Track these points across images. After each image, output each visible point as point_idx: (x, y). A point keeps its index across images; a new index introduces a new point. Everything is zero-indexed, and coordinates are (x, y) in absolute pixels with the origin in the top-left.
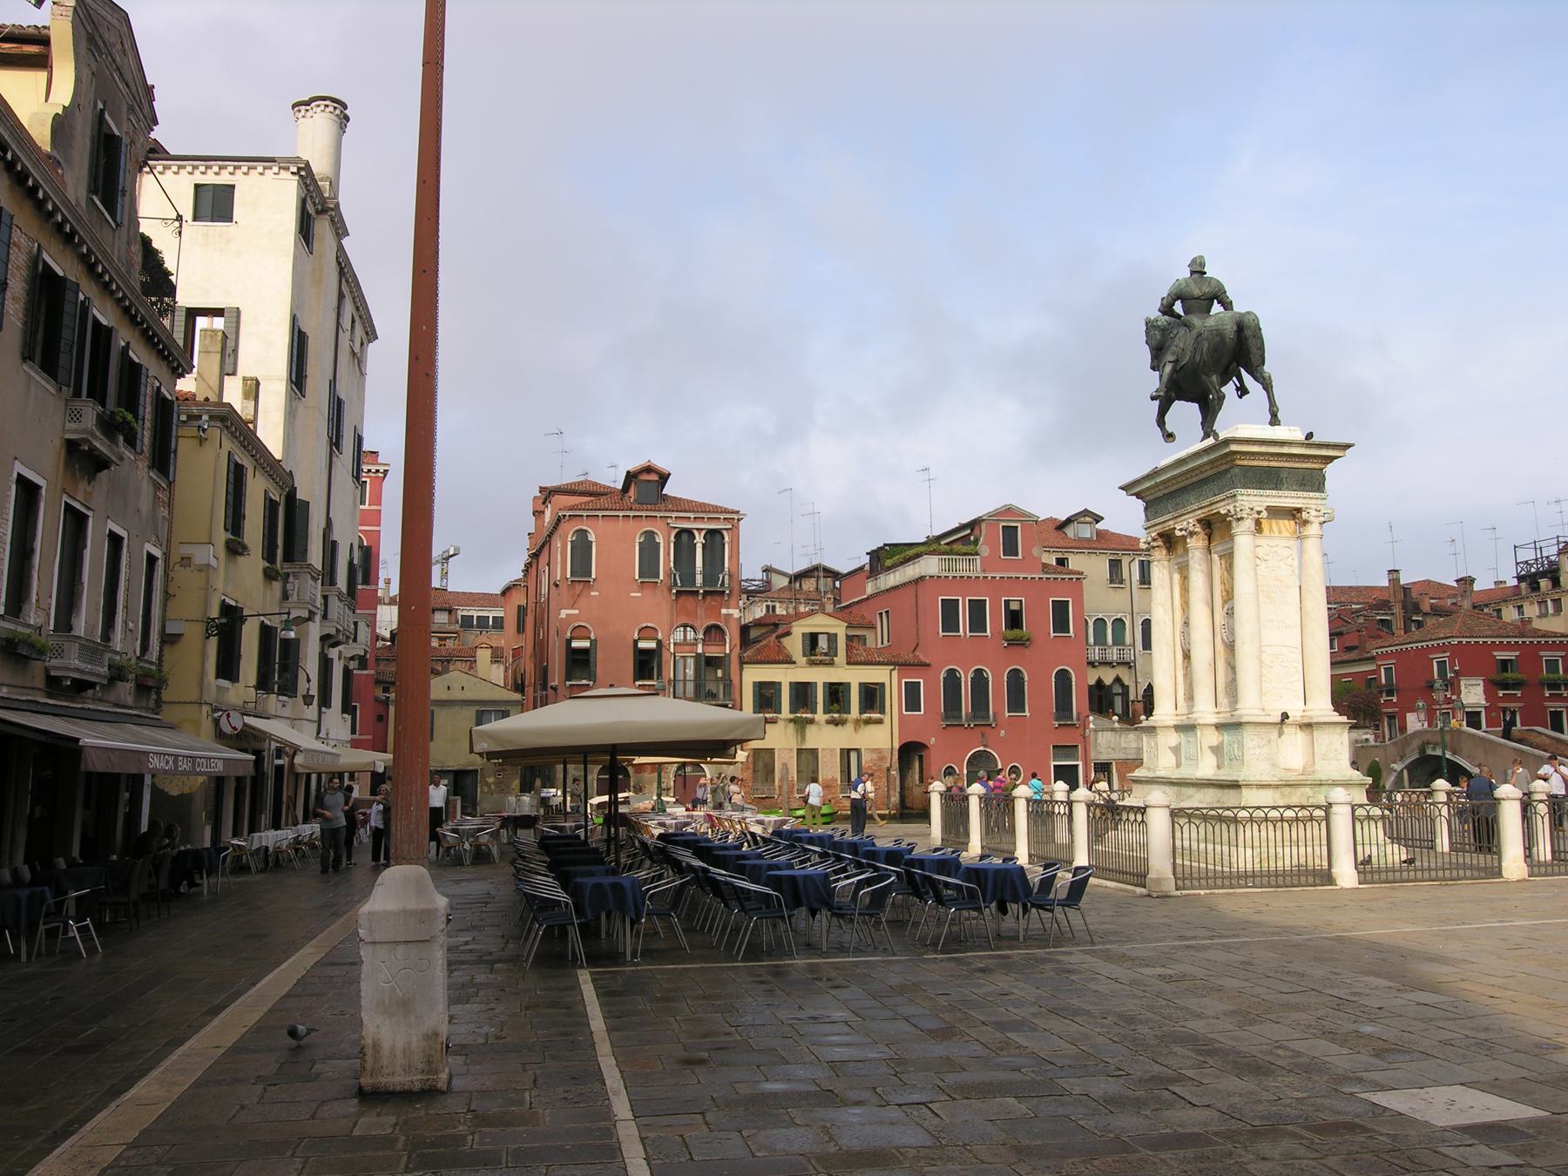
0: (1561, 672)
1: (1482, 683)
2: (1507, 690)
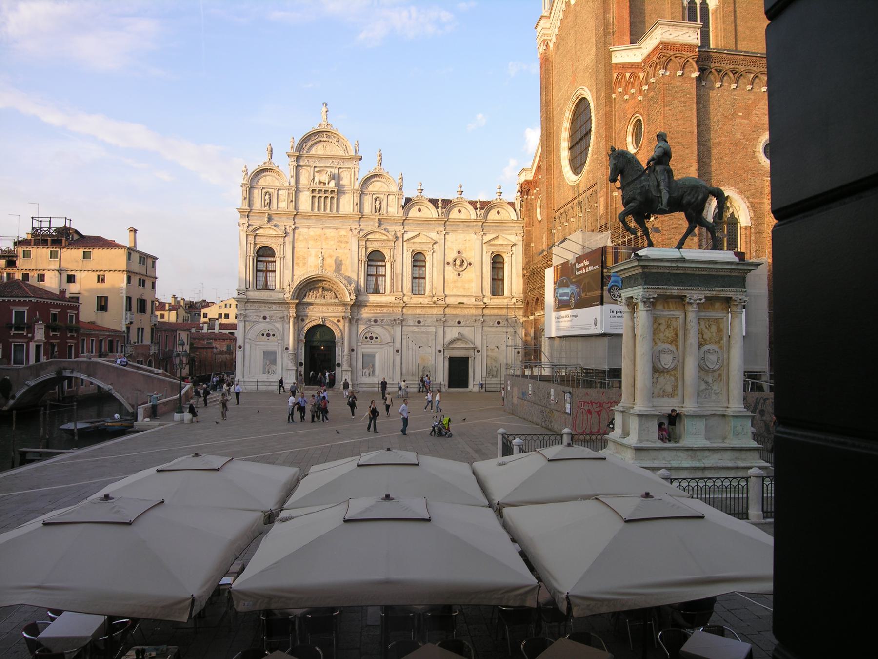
0: (74, 323)
1: (43, 327)
2: (54, 332)
